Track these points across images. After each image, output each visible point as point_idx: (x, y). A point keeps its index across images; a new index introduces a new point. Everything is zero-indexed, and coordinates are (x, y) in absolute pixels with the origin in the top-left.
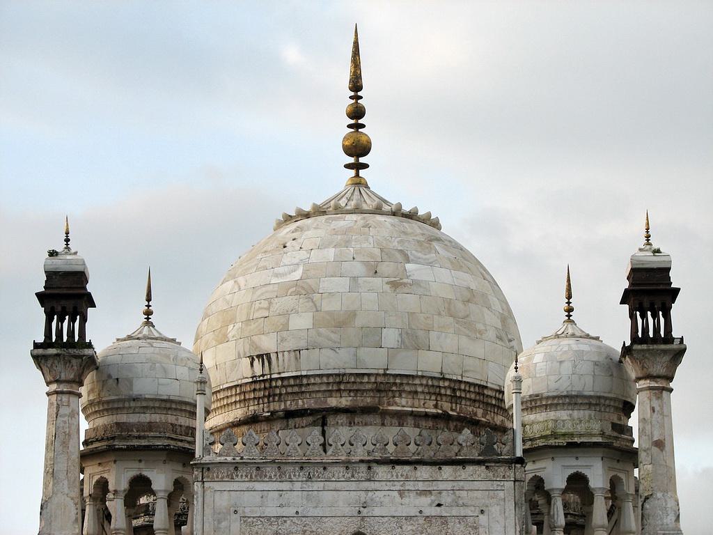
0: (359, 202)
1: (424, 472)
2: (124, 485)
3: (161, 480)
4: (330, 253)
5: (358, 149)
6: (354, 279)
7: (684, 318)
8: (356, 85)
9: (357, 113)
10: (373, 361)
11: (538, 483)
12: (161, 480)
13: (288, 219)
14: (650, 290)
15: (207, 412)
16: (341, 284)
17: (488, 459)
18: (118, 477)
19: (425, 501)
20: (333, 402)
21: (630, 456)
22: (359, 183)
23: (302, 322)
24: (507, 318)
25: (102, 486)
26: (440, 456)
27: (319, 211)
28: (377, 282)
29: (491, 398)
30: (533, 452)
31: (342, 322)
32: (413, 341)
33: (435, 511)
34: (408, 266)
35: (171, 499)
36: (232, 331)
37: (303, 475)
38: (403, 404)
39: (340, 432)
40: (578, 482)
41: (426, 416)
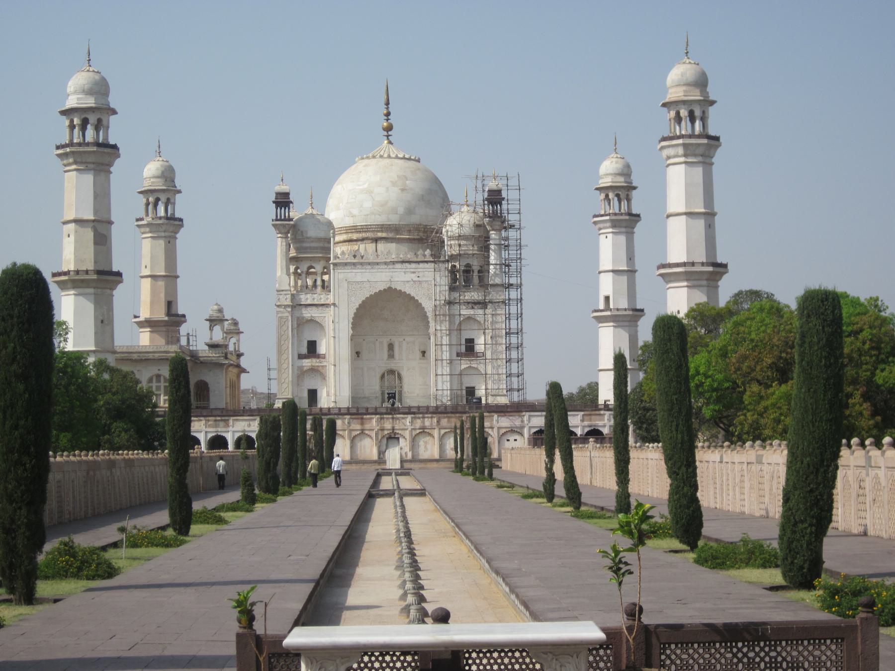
1: (413, 265)
2: (305, 269)
3: (318, 268)
6: (387, 188)
8: (387, 104)
9: (388, 114)
10: (394, 220)
14: (495, 198)
15: (334, 237)
17: (436, 258)
19: (413, 276)
20: (380, 235)
22: (390, 143)
23: (368, 204)
26: (419, 260)
30: (452, 258)
32: (410, 211)
33: (417, 279)
34: (407, 182)
37: (369, 267)
39: (381, 246)
40: (468, 265)
41: (414, 239)
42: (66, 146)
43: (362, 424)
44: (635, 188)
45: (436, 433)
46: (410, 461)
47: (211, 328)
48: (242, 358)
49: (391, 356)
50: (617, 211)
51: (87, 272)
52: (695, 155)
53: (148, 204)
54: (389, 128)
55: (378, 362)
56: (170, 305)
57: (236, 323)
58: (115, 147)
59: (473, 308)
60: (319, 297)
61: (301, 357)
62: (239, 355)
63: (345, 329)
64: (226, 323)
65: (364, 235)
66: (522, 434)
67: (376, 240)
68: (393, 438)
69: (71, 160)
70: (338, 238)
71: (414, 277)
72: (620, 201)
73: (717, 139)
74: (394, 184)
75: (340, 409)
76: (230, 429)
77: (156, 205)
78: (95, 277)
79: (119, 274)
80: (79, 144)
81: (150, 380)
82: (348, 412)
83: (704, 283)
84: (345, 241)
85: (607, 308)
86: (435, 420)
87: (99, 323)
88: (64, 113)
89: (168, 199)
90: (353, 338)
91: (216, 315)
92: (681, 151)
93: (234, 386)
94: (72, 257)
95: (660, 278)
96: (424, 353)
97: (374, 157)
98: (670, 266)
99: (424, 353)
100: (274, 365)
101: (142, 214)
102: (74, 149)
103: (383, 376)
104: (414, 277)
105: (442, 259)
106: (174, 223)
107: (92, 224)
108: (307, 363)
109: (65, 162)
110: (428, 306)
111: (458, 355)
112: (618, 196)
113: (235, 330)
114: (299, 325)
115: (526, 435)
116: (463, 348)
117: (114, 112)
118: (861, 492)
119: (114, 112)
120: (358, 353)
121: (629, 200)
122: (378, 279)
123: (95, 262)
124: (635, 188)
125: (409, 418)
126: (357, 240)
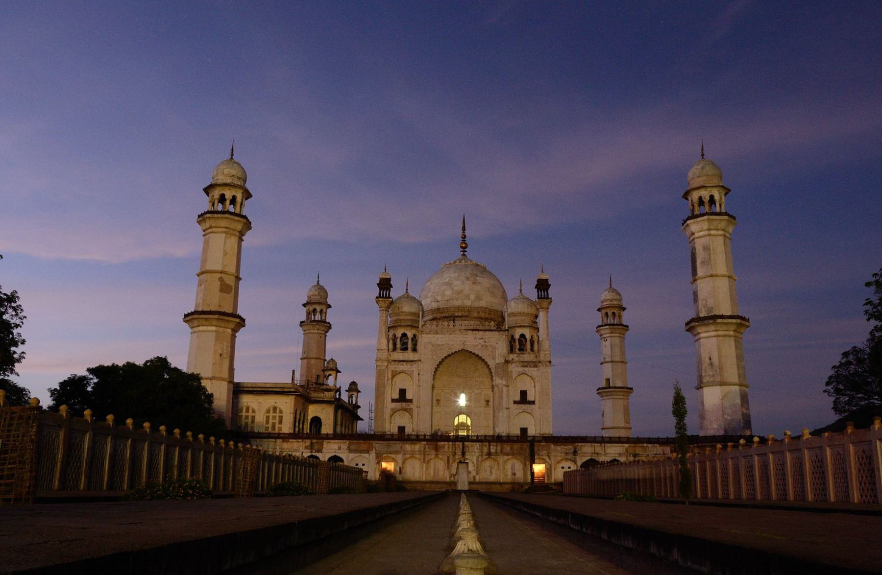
1: (481, 332)
8: (464, 229)
9: (464, 237)
10: (468, 303)
11: (512, 336)
12: (410, 335)
21: (538, 329)
22: (464, 255)
23: (448, 293)
25: (395, 335)
31: (460, 292)
32: (478, 298)
35: (412, 339)
36: (429, 295)
38: (475, 314)
40: (523, 336)
41: (481, 318)
42: (205, 213)
43: (437, 449)
44: (624, 309)
46: (478, 483)
52: (717, 230)
53: (308, 313)
54: (466, 248)
59: (526, 366)
60: (409, 355)
61: (393, 401)
63: (427, 377)
69: (208, 225)
75: (418, 436)
76: (324, 450)
78: (216, 316)
81: (268, 411)
83: (732, 333)
84: (430, 320)
86: (499, 448)
87: (218, 356)
89: (322, 310)
94: (201, 301)
95: (689, 333)
99: (488, 401)
101: (304, 318)
105: (503, 328)
107: (219, 275)
109: (204, 228)
111: (515, 402)
113: (353, 387)
114: (393, 377)
115: (579, 463)
116: (518, 398)
121: (620, 317)
123: (220, 306)
124: (624, 309)
125: (477, 445)
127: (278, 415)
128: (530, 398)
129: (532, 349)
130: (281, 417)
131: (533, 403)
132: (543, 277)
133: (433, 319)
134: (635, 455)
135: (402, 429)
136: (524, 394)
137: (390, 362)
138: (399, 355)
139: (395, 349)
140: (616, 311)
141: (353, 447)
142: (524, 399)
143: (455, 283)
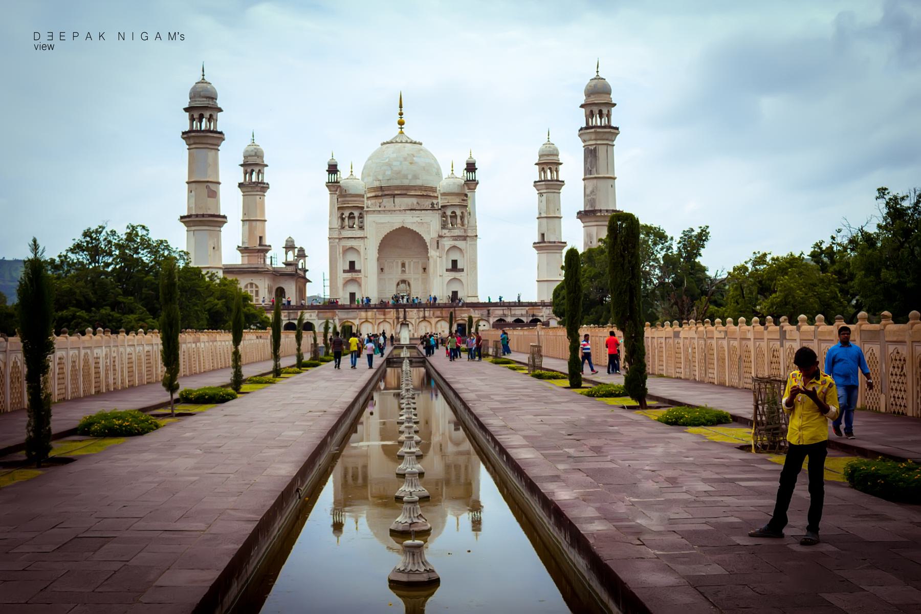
0: (401, 140)
4: (395, 155)
5: (401, 123)
7: (478, 175)
8: (401, 107)
9: (401, 114)
10: (406, 182)
12: (356, 214)
13: (384, 143)
14: (471, 167)
16: (398, 163)
17: (433, 209)
18: (346, 214)
20: (396, 192)
23: (389, 173)
24: (439, 169)
25: (343, 214)
27: (392, 142)
28: (407, 163)
29: (433, 189)
31: (399, 173)
38: (413, 193)
39: (397, 200)
45: (433, 321)
47: (286, 253)
48: (307, 273)
49: (404, 272)
50: (549, 178)
51: (203, 216)
53: (245, 173)
55: (395, 274)
56: (261, 238)
57: (301, 250)
58: (221, 133)
61: (345, 271)
62: (305, 271)
64: (296, 250)
65: (386, 193)
66: (488, 321)
67: (394, 196)
68: (405, 324)
70: (369, 195)
71: (418, 219)
72: (551, 172)
73: (617, 129)
74: (405, 159)
77: (251, 174)
79: (224, 217)
80: (197, 131)
81: (246, 286)
82: (375, 307)
85: (543, 241)
88: (186, 110)
90: (378, 259)
91: (289, 244)
92: (593, 137)
93: (301, 291)
96: (425, 269)
97: (392, 142)
98: (585, 211)
99: (425, 269)
100: (327, 276)
102: (193, 134)
103: (398, 284)
104: (418, 219)
106: (262, 187)
108: (349, 275)
110: (427, 238)
111: (447, 270)
112: (550, 169)
113: (302, 254)
115: (491, 322)
116: (450, 267)
117: (220, 110)
118: (774, 360)
119: (220, 110)
120: (382, 269)
121: (557, 171)
122: (396, 221)
126: (382, 196)
127: (254, 289)
128: (459, 266)
129: (463, 225)
130: (257, 292)
131: (462, 270)
132: (471, 161)
133: (376, 196)
134: (533, 315)
135: (352, 295)
136: (454, 263)
137: (340, 239)
138: (347, 233)
139: (343, 228)
140: (554, 168)
141: (321, 315)
142: (454, 266)
143: (395, 163)
